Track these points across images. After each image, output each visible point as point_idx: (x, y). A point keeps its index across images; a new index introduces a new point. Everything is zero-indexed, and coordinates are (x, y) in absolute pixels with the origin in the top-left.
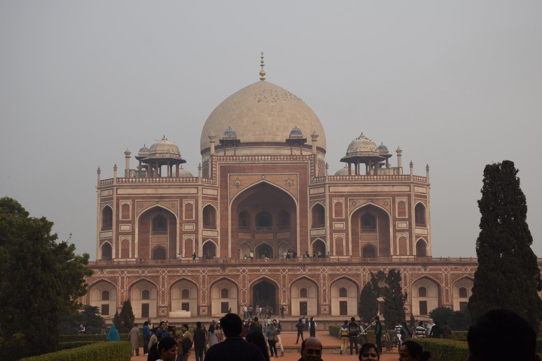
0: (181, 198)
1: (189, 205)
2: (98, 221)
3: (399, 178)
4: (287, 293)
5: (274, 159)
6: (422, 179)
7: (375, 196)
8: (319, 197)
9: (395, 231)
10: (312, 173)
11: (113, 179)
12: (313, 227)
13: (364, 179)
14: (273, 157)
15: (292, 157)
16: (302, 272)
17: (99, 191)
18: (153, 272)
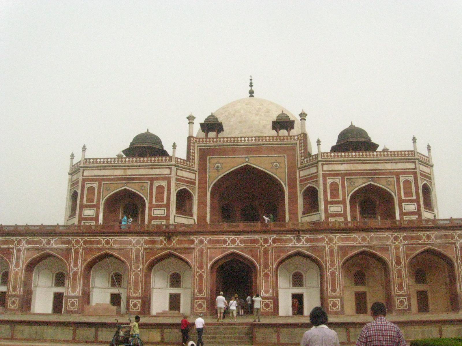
0: (152, 179)
1: (160, 188)
2: (66, 208)
3: (401, 154)
4: (270, 279)
5: (259, 140)
6: (425, 157)
7: (376, 174)
8: (311, 178)
9: (402, 214)
10: (301, 153)
11: (80, 161)
12: (304, 213)
13: (363, 155)
14: (257, 138)
15: (278, 138)
16: (294, 244)
17: (70, 176)
18: (63, 243)
